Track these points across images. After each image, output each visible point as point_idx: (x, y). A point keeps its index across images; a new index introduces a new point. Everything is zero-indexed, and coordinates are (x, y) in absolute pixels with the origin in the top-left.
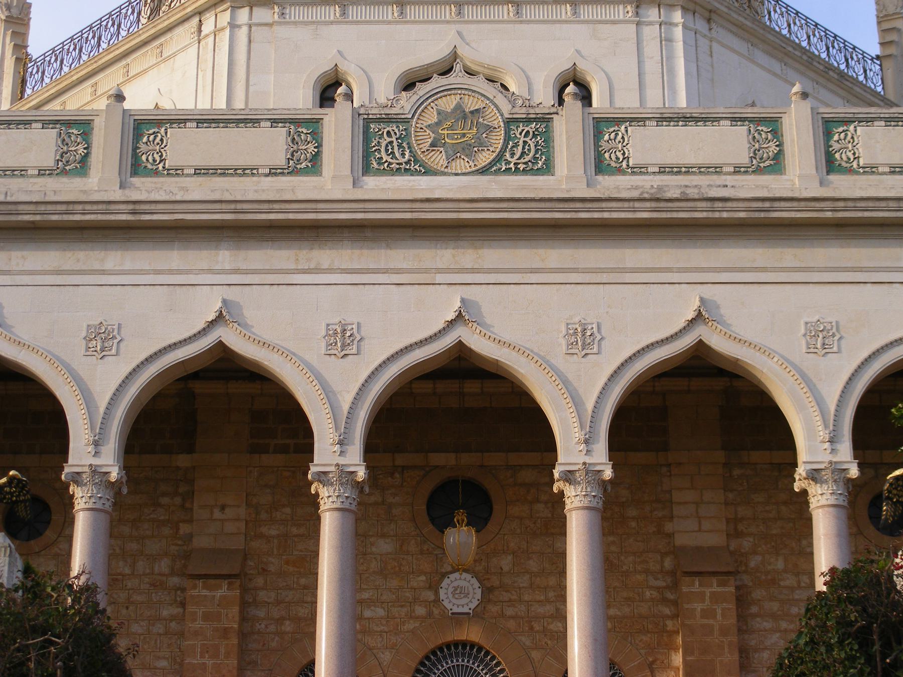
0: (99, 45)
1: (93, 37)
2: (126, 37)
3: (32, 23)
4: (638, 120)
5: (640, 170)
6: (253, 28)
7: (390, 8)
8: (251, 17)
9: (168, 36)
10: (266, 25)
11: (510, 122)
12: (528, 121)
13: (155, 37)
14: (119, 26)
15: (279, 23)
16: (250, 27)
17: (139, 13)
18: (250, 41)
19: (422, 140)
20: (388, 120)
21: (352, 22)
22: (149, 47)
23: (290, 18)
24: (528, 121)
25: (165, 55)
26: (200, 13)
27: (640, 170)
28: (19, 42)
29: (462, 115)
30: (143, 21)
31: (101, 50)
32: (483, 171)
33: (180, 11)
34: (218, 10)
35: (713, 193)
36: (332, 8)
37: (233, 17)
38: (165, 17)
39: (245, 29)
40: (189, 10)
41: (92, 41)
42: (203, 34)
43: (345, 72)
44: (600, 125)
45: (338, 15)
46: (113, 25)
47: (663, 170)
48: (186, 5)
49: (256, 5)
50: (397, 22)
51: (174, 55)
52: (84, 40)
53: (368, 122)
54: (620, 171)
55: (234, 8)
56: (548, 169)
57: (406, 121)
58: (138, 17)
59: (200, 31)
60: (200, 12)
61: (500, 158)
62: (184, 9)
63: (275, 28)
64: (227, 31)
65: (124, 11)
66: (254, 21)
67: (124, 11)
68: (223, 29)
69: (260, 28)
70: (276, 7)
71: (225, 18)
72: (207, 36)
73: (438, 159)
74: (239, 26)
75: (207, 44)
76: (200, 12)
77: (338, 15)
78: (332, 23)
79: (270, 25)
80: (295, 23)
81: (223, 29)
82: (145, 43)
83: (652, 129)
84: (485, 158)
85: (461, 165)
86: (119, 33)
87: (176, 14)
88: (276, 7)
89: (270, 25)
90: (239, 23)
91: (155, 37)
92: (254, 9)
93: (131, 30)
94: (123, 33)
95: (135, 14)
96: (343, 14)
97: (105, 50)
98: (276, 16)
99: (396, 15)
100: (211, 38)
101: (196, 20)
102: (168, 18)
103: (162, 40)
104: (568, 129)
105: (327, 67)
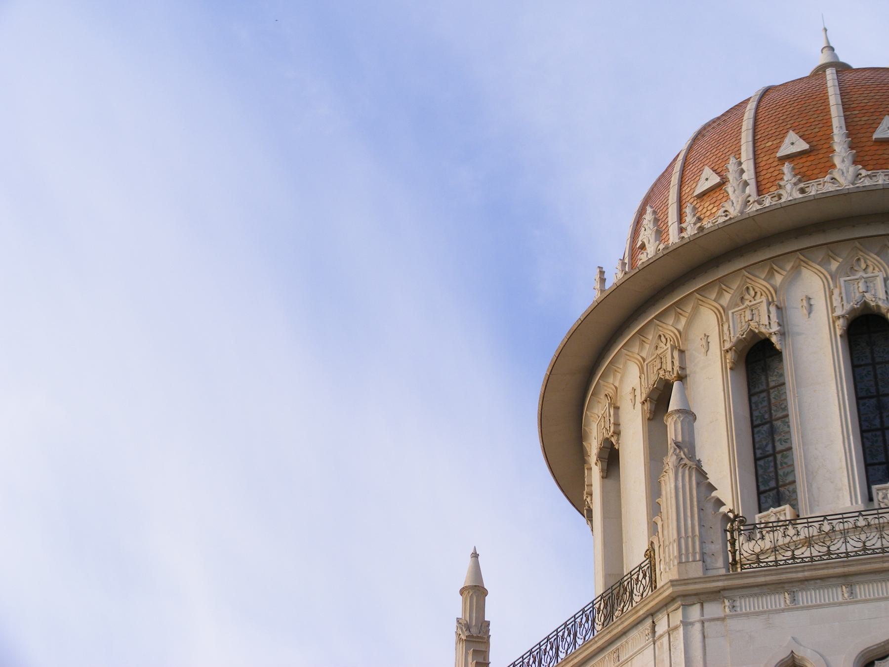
0: (557, 655)
1: (551, 648)
2: (583, 645)
3: (492, 640)
6: (706, 624)
7: (839, 590)
8: (702, 614)
9: (623, 641)
10: (718, 619)
13: (611, 642)
14: (575, 635)
15: (732, 617)
16: (703, 623)
17: (593, 621)
18: (704, 637)
21: (803, 608)
22: (605, 653)
23: (741, 609)
25: (622, 659)
26: (652, 615)
28: (481, 660)
30: (598, 627)
31: (559, 660)
33: (634, 614)
34: (670, 610)
36: (782, 597)
37: (685, 615)
38: (619, 622)
39: (698, 626)
40: (641, 612)
41: (551, 652)
42: (657, 635)
43: (802, 659)
45: (788, 602)
46: (569, 635)
48: (638, 608)
49: (707, 601)
50: (848, 603)
51: (631, 658)
52: (542, 652)
55: (685, 606)
58: (593, 624)
59: (654, 632)
60: (652, 614)
62: (637, 612)
63: (728, 621)
64: (681, 629)
65: (578, 620)
66: (706, 617)
67: (578, 620)
68: (676, 628)
69: (712, 623)
70: (727, 603)
71: (677, 617)
72: (661, 636)
74: (692, 624)
75: (662, 644)
76: (652, 614)
77: (788, 602)
78: (783, 610)
79: (723, 619)
80: (747, 615)
81: (676, 628)
82: (601, 649)
86: (576, 641)
87: (629, 618)
88: (727, 603)
89: (723, 619)
90: (691, 620)
91: (611, 642)
92: (705, 605)
93: (587, 638)
94: (580, 642)
95: (590, 622)
96: (794, 600)
97: (563, 660)
98: (727, 610)
99: (846, 595)
100: (666, 639)
101: (649, 622)
102: (622, 623)
103: (618, 644)
105: (783, 655)
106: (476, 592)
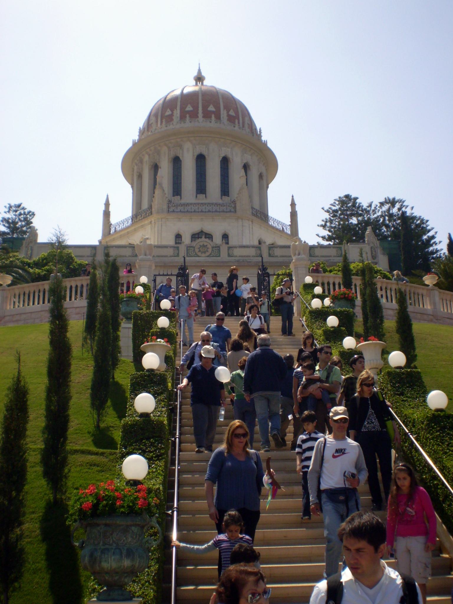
4: (236, 247)
5: (236, 256)
11: (213, 247)
12: (216, 247)
19: (197, 250)
20: (191, 247)
24: (216, 247)
27: (236, 256)
29: (204, 246)
32: (208, 256)
35: (249, 261)
44: (229, 248)
47: (240, 256)
53: (187, 247)
54: (232, 256)
56: (219, 256)
57: (194, 247)
61: (211, 254)
73: (199, 254)
83: (238, 249)
84: (207, 254)
85: (203, 255)
104: (224, 249)
106: (107, 204)
